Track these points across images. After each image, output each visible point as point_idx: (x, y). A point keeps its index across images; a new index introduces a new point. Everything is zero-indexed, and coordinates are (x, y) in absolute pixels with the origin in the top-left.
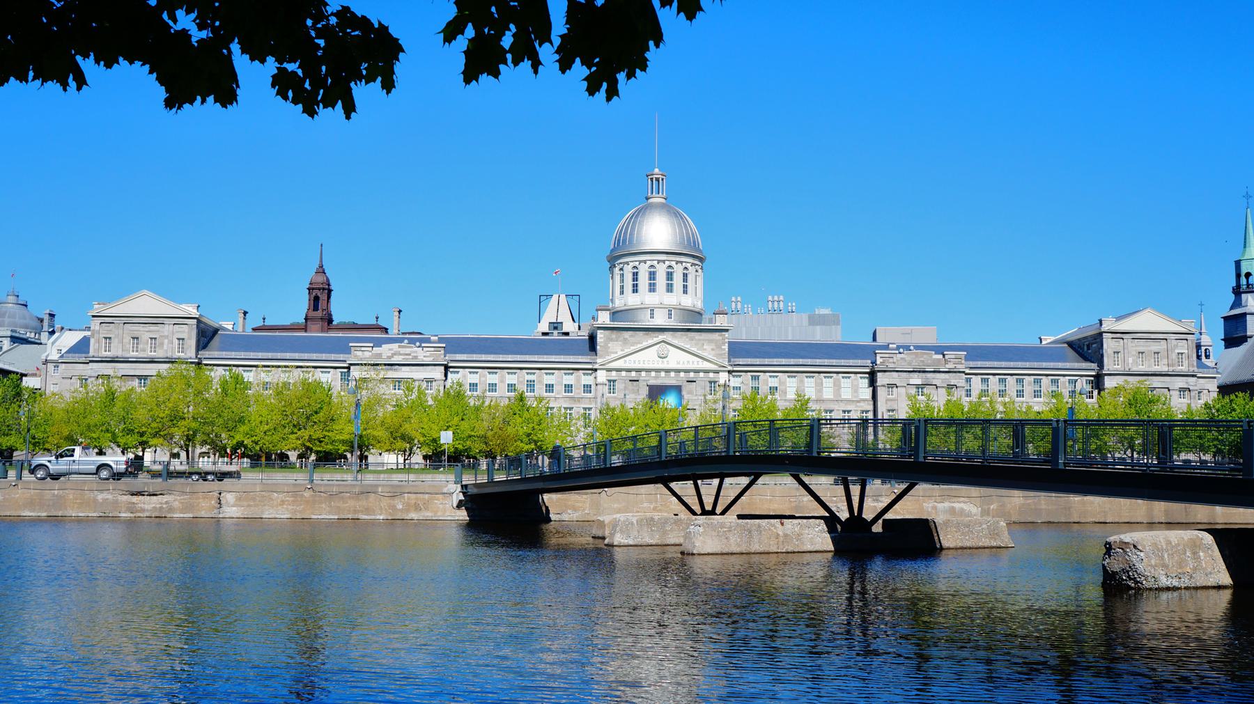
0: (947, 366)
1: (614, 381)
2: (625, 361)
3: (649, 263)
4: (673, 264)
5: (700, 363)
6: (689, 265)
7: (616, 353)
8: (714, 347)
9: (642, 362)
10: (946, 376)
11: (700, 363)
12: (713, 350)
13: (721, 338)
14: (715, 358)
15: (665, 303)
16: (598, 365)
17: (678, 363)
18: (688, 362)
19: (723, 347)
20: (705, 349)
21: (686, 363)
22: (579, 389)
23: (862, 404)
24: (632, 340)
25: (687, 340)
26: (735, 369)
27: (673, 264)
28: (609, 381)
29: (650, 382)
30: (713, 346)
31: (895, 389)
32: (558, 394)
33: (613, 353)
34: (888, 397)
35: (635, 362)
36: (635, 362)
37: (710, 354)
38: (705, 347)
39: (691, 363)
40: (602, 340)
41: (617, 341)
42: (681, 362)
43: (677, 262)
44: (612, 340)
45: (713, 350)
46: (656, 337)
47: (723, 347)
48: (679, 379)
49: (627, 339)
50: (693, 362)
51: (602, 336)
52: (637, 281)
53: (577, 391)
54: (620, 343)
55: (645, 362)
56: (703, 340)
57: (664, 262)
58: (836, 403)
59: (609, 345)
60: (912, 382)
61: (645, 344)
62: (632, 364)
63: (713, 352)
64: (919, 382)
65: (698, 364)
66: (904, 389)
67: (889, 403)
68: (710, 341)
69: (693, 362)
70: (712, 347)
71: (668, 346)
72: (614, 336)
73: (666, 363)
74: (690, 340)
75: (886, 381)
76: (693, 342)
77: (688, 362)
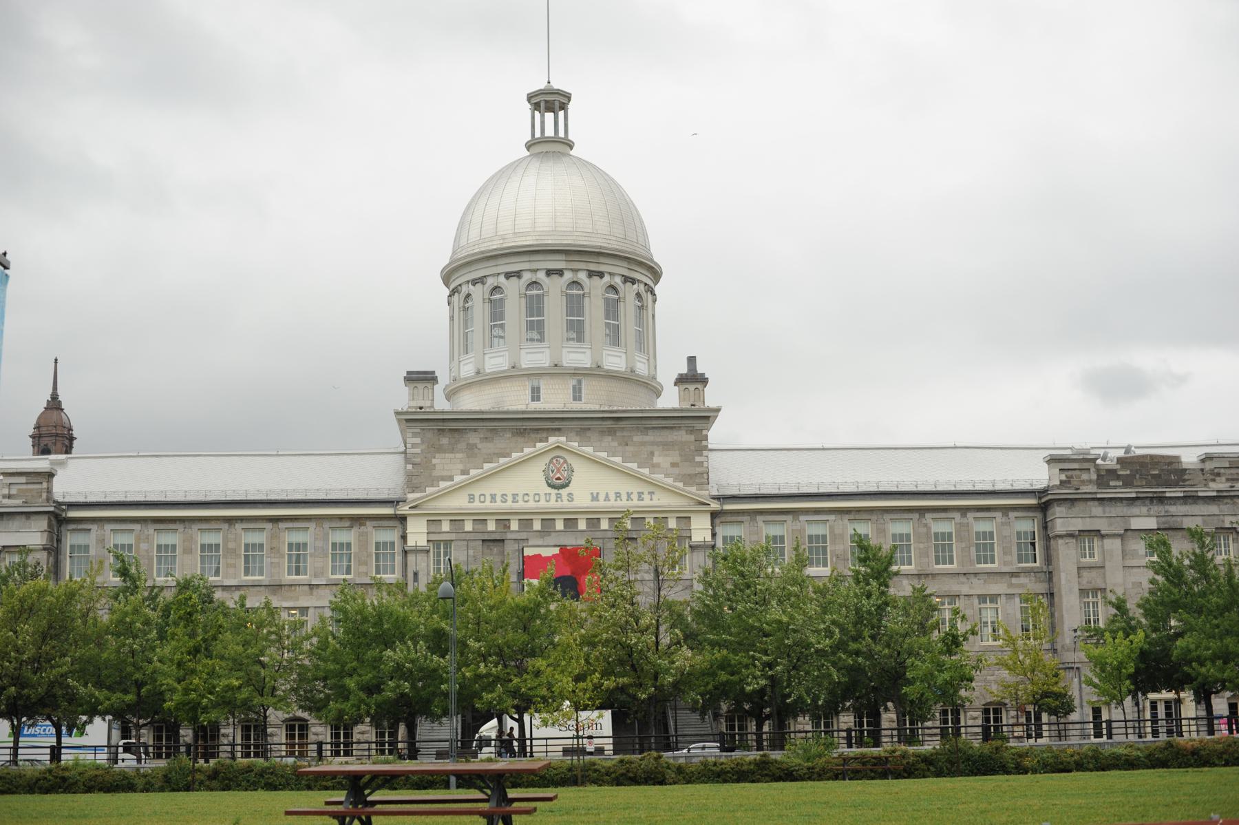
0: (1213, 485)
1: (448, 543)
2: (471, 498)
3: (527, 277)
4: (582, 276)
5: (646, 497)
6: (618, 280)
7: (451, 478)
8: (677, 459)
9: (510, 499)
10: (1213, 509)
11: (646, 497)
12: (674, 465)
13: (692, 438)
14: (680, 485)
15: (565, 365)
16: (407, 508)
17: (595, 498)
18: (618, 495)
20: (657, 466)
21: (612, 497)
22: (366, 564)
23: (1023, 580)
24: (487, 448)
25: (615, 444)
26: (727, 507)
27: (582, 276)
28: (437, 543)
30: (675, 457)
31: (1096, 542)
32: (316, 576)
33: (444, 479)
34: (1083, 560)
35: (493, 497)
36: (493, 497)
37: (667, 475)
38: (656, 460)
39: (624, 497)
40: (418, 451)
42: (601, 497)
43: (591, 274)
44: (440, 449)
45: (674, 465)
46: (541, 441)
48: (599, 534)
49: (475, 445)
50: (629, 495)
51: (418, 440)
52: (502, 318)
53: (363, 569)
54: (460, 455)
55: (520, 498)
56: (653, 443)
57: (560, 272)
58: (963, 579)
59: (434, 461)
60: (1136, 524)
63: (676, 471)
64: (1151, 523)
65: (640, 498)
66: (1118, 542)
67: (1085, 573)
68: (667, 446)
69: (629, 495)
70: (670, 459)
71: (572, 460)
72: (445, 441)
73: (565, 498)
74: (620, 444)
75: (1077, 525)
76: (630, 449)
77: (618, 495)
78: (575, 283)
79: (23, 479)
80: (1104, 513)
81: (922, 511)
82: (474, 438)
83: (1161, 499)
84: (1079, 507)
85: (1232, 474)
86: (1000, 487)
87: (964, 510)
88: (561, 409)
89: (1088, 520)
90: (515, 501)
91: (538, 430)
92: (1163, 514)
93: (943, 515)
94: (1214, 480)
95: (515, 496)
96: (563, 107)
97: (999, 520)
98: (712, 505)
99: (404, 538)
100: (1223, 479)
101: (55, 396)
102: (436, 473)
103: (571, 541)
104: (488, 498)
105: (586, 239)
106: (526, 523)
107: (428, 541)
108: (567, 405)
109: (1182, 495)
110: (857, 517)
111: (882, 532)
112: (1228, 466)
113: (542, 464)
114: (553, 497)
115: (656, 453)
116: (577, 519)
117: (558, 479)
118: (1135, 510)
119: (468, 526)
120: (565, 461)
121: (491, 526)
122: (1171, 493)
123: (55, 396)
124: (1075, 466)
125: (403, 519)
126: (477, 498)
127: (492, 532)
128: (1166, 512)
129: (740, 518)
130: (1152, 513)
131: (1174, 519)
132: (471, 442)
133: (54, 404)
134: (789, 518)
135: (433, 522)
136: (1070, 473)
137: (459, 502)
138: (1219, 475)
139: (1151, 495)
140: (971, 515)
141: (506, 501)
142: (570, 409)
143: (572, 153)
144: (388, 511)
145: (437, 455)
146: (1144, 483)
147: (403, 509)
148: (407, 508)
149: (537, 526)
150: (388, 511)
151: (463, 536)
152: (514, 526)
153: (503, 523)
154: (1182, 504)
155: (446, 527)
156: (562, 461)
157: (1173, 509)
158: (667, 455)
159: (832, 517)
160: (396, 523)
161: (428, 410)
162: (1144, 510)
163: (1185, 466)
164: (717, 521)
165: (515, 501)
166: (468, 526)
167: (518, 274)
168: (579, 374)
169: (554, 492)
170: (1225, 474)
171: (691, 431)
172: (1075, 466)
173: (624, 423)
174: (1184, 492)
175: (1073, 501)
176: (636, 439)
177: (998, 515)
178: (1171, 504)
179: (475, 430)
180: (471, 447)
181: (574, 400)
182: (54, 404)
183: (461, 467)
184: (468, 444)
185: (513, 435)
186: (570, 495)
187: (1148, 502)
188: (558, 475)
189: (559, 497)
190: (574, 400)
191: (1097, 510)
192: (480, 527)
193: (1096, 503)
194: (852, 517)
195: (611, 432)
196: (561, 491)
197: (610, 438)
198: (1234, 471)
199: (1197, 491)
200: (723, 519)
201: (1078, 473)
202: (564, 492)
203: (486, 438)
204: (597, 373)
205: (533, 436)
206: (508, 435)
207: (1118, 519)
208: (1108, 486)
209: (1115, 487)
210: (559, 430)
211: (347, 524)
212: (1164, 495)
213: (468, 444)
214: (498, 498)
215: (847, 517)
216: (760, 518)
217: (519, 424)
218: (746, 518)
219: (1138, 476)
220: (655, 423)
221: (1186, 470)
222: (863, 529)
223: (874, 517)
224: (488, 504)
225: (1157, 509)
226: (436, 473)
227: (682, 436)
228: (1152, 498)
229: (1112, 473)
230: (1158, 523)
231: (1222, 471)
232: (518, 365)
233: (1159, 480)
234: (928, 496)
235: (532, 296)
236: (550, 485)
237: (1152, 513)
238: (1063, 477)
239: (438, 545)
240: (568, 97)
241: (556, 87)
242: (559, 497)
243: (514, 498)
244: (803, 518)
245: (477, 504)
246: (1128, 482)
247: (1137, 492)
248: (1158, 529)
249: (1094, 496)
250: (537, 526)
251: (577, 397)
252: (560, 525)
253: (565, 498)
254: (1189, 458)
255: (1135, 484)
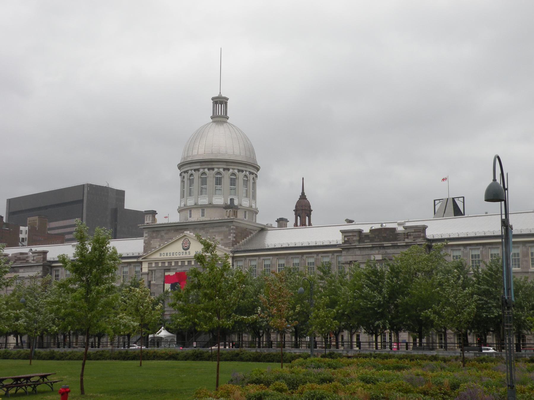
2: (161, 255)
9: (172, 254)
10: (405, 250)
13: (227, 229)
14: (223, 247)
16: (141, 259)
19: (229, 237)
24: (166, 236)
25: (204, 233)
28: (152, 271)
29: (178, 270)
33: (153, 248)
36: (167, 255)
41: (156, 238)
46: (182, 233)
47: (229, 237)
54: (158, 240)
55: (174, 254)
59: (152, 242)
61: (175, 239)
62: (181, 255)
70: (220, 238)
72: (154, 235)
73: (188, 253)
74: (205, 233)
78: (204, 173)
79: (36, 254)
80: (361, 253)
81: (303, 254)
82: (163, 233)
83: (384, 247)
84: (351, 252)
85: (416, 235)
86: (319, 244)
87: (318, 253)
88: (196, 221)
89: (354, 256)
90: (173, 255)
91: (181, 229)
92: (384, 253)
93: (310, 255)
94: (408, 238)
95: (173, 253)
96: (226, 103)
97: (330, 257)
98: (230, 254)
99: (142, 269)
100: (412, 237)
101: (303, 193)
102: (152, 246)
103: (180, 270)
104: (165, 255)
105: (208, 156)
106: (176, 263)
107: (149, 270)
108: (199, 219)
109: (391, 245)
110: (280, 257)
111: (288, 262)
112: (413, 231)
113: (181, 242)
114: (184, 253)
115: (216, 236)
116: (191, 261)
117: (186, 246)
118: (373, 252)
119: (160, 265)
120: (188, 240)
121: (167, 264)
122: (386, 244)
123: (303, 193)
124: (351, 234)
125: (141, 263)
126: (162, 255)
127: (167, 266)
128: (386, 252)
129: (241, 259)
130: (380, 253)
131: (389, 255)
132: (162, 235)
133: (303, 196)
134: (257, 258)
135: (150, 264)
136: (349, 237)
137: (157, 256)
138: (410, 235)
139: (378, 245)
140: (320, 255)
141: (171, 255)
142: (190, 221)
143: (228, 121)
144: (135, 260)
145: (152, 240)
146: (379, 240)
147: (140, 260)
148: (141, 259)
149: (180, 264)
150: (135, 260)
151: (158, 268)
152: (173, 264)
153: (170, 263)
154: (392, 249)
155: (154, 265)
156: (187, 240)
157: (389, 251)
158: (220, 236)
159: (271, 258)
160: (139, 264)
161: (151, 224)
162: (377, 252)
163: (398, 232)
164: (235, 260)
165: (173, 255)
166: (160, 265)
167: (198, 170)
168: (203, 208)
169: (185, 251)
170: (413, 235)
171: (227, 227)
172: (351, 234)
173: (207, 225)
174: (392, 243)
175: (349, 249)
176: (211, 230)
177: (330, 255)
178: (388, 249)
179: (163, 230)
180: (162, 236)
181: (202, 216)
182: (303, 196)
183: (158, 243)
184: (161, 236)
185: (174, 231)
186: (189, 252)
187: (378, 248)
188: (186, 245)
189: (186, 253)
190: (202, 216)
191: (358, 252)
192: (163, 265)
193: (358, 249)
194: (278, 257)
195: (203, 229)
196: (187, 251)
197: (203, 231)
198: (417, 233)
199: (397, 243)
200: (236, 259)
201: (352, 237)
202: (187, 251)
203: (166, 233)
204: (211, 206)
205: (180, 231)
206: (173, 231)
207: (366, 256)
208: (364, 242)
209: (366, 242)
210: (187, 229)
211: (126, 265)
212: (383, 245)
213: (161, 236)
214: (168, 254)
215: (277, 257)
216: (248, 259)
217: (175, 227)
218: (243, 259)
219: (377, 237)
220: (217, 225)
221: (399, 233)
222: (282, 262)
223: (286, 257)
224: (165, 256)
225: (382, 251)
226: (152, 246)
227: (225, 229)
228: (380, 247)
229: (367, 236)
230: (382, 257)
231: (412, 233)
232: (197, 204)
233: (386, 239)
234: (296, 248)
235: (203, 178)
236: (184, 249)
237: (380, 253)
238: (346, 239)
239: (151, 272)
240: (227, 99)
241: (223, 96)
242: (186, 253)
243: (173, 254)
244: (262, 258)
245: (162, 257)
246: (372, 240)
247: (372, 244)
248: (382, 260)
249: (355, 247)
250: (180, 264)
251: (203, 215)
252: (186, 263)
253: (188, 253)
254: (400, 229)
255: (375, 241)
